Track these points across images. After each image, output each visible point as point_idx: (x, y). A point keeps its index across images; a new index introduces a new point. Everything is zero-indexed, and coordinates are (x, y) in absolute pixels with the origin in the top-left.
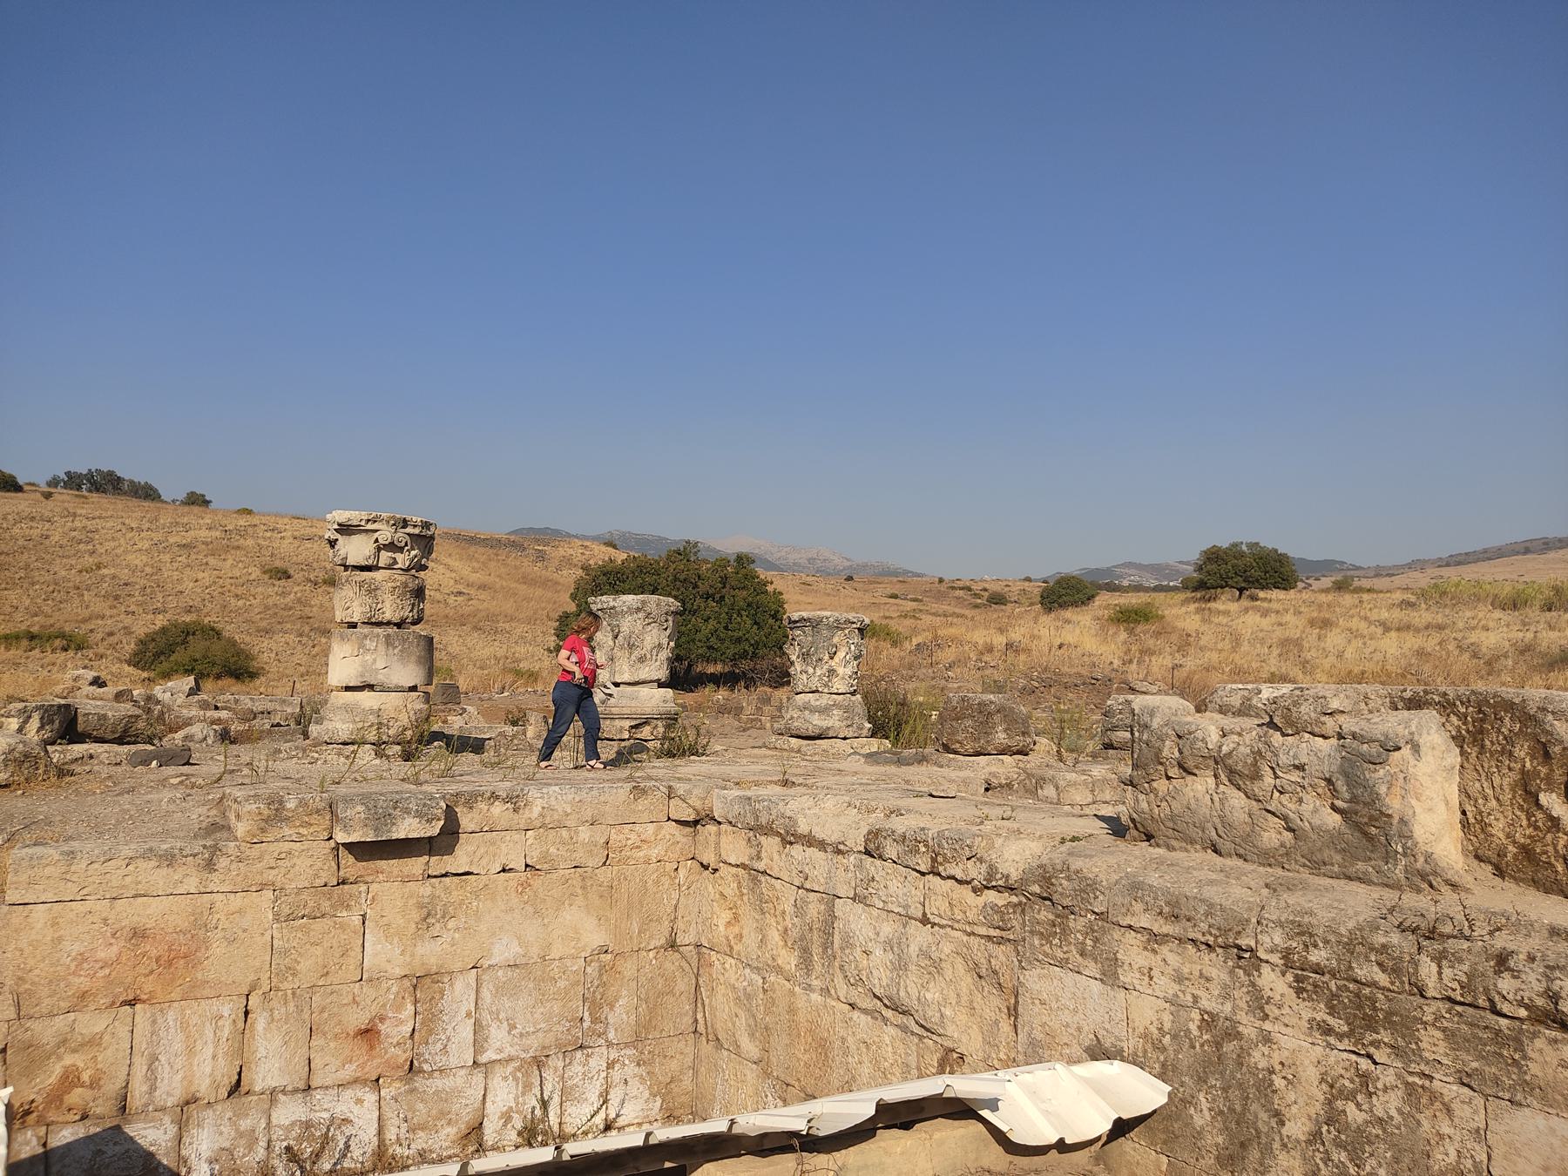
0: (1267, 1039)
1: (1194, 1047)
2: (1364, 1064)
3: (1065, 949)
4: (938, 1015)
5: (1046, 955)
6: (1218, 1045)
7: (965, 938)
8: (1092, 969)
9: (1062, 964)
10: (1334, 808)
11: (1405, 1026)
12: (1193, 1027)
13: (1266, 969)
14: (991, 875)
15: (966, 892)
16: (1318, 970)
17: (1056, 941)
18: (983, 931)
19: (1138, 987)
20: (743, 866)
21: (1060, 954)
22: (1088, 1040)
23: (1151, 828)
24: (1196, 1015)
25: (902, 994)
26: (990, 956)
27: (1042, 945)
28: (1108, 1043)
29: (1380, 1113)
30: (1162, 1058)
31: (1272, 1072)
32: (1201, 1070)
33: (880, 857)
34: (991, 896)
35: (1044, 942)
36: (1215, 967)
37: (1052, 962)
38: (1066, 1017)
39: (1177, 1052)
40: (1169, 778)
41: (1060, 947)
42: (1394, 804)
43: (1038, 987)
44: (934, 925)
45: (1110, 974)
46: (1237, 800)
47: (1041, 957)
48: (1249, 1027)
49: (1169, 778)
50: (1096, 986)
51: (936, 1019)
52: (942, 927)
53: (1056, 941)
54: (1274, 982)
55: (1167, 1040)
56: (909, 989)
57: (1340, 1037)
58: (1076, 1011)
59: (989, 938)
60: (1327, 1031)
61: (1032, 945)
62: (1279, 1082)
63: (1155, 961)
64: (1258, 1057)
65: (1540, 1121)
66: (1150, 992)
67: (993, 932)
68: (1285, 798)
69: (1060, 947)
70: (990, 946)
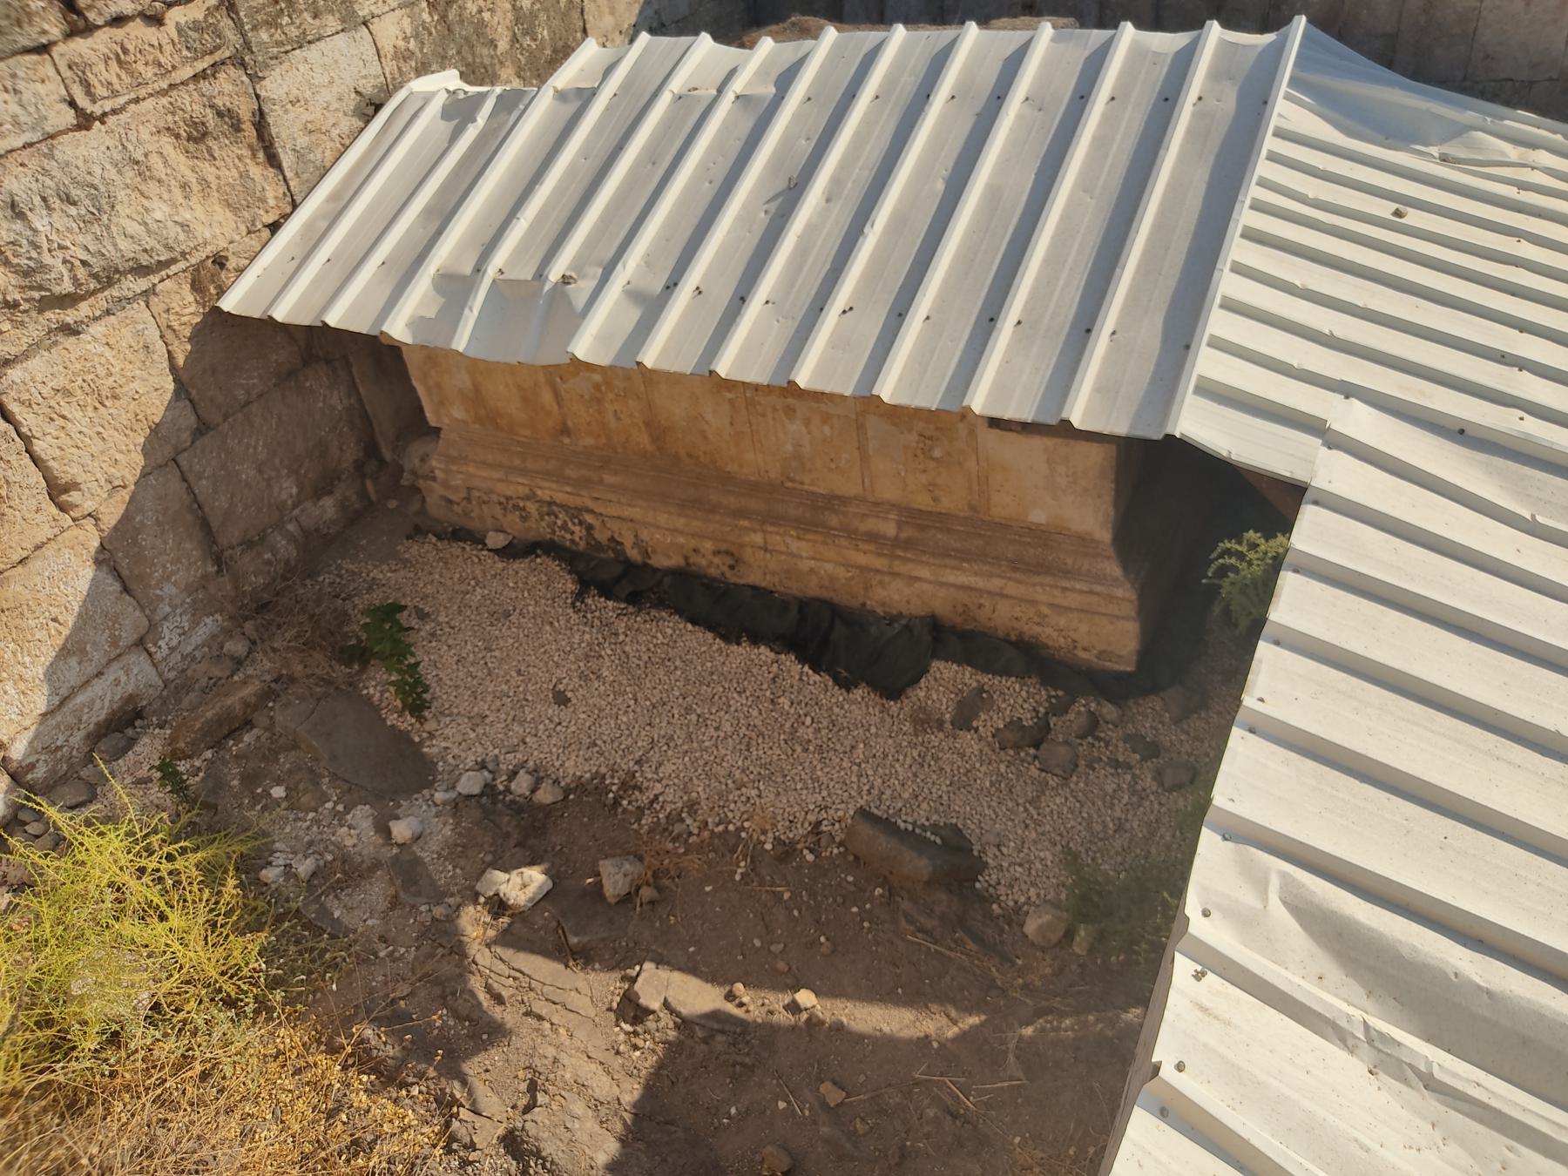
1: (430, 34)
3: (298, 22)
4: (179, 229)
5: (279, 44)
6: (443, 18)
7: (164, 101)
8: (332, 23)
9: (303, 42)
12: (426, 16)
17: (286, 20)
18: (186, 72)
19: (376, 12)
21: (294, 32)
22: (352, 101)
25: (124, 244)
26: (211, 98)
27: (271, 36)
28: (368, 88)
30: (413, 64)
31: (480, 11)
32: (440, 50)
35: (273, 30)
37: (289, 48)
38: (326, 96)
39: (421, 50)
41: (293, 23)
43: (286, 89)
44: (102, 118)
47: (275, 50)
51: (182, 237)
52: (122, 109)
53: (286, 20)
55: (412, 44)
56: (129, 231)
58: (331, 83)
61: (261, 43)
62: (486, 15)
66: (387, 9)
67: (201, 65)
69: (293, 23)
70: (204, 85)
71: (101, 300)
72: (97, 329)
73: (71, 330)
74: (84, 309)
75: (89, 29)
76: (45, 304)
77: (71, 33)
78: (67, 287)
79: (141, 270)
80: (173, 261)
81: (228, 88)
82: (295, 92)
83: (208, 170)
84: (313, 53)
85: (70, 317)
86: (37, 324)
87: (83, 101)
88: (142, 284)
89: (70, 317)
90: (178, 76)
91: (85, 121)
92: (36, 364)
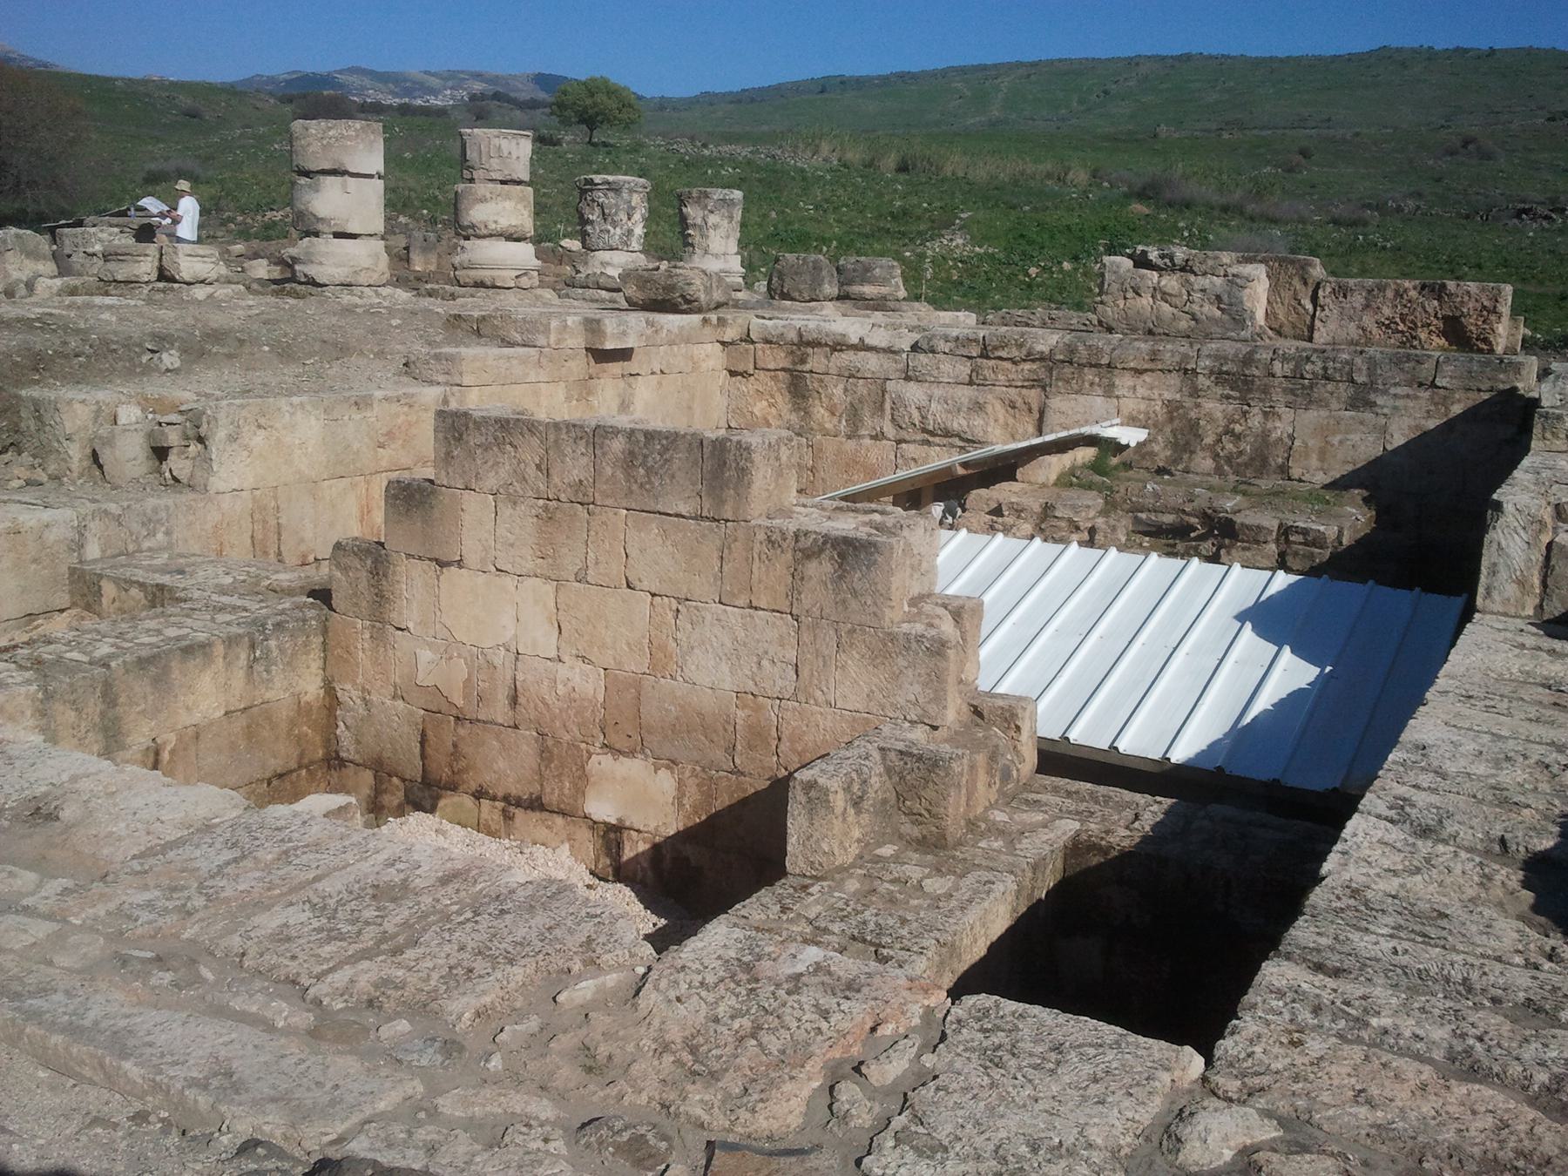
0: (1198, 406)
2: (1246, 407)
8: (1100, 392)
10: (1218, 308)
11: (1265, 390)
12: (1158, 408)
13: (1200, 377)
14: (1029, 354)
15: (1008, 365)
16: (1227, 373)
18: (1020, 384)
20: (783, 369)
23: (1114, 325)
24: (1160, 403)
29: (1250, 425)
33: (933, 352)
34: (1027, 366)
36: (1174, 379)
40: (1125, 298)
42: (1248, 305)
45: (1109, 392)
46: (1166, 307)
48: (1189, 402)
49: (1125, 298)
50: (1099, 400)
51: (981, 434)
54: (1203, 381)
57: (1235, 399)
59: (1023, 387)
60: (1228, 397)
62: (1202, 423)
63: (1139, 382)
64: (1193, 415)
65: (1315, 414)
68: (1193, 306)
70: (1024, 391)
71: (945, 441)
72: (938, 448)
73: (928, 443)
74: (937, 440)
75: (988, 358)
76: (924, 430)
77: (981, 356)
78: (931, 428)
79: (962, 439)
80: (974, 442)
81: (1033, 395)
82: (1063, 409)
83: (1011, 421)
84: (1081, 399)
85: (931, 439)
86: (920, 436)
87: (974, 378)
88: (962, 444)
89: (931, 439)
90: (1014, 383)
91: (971, 383)
92: (912, 447)
